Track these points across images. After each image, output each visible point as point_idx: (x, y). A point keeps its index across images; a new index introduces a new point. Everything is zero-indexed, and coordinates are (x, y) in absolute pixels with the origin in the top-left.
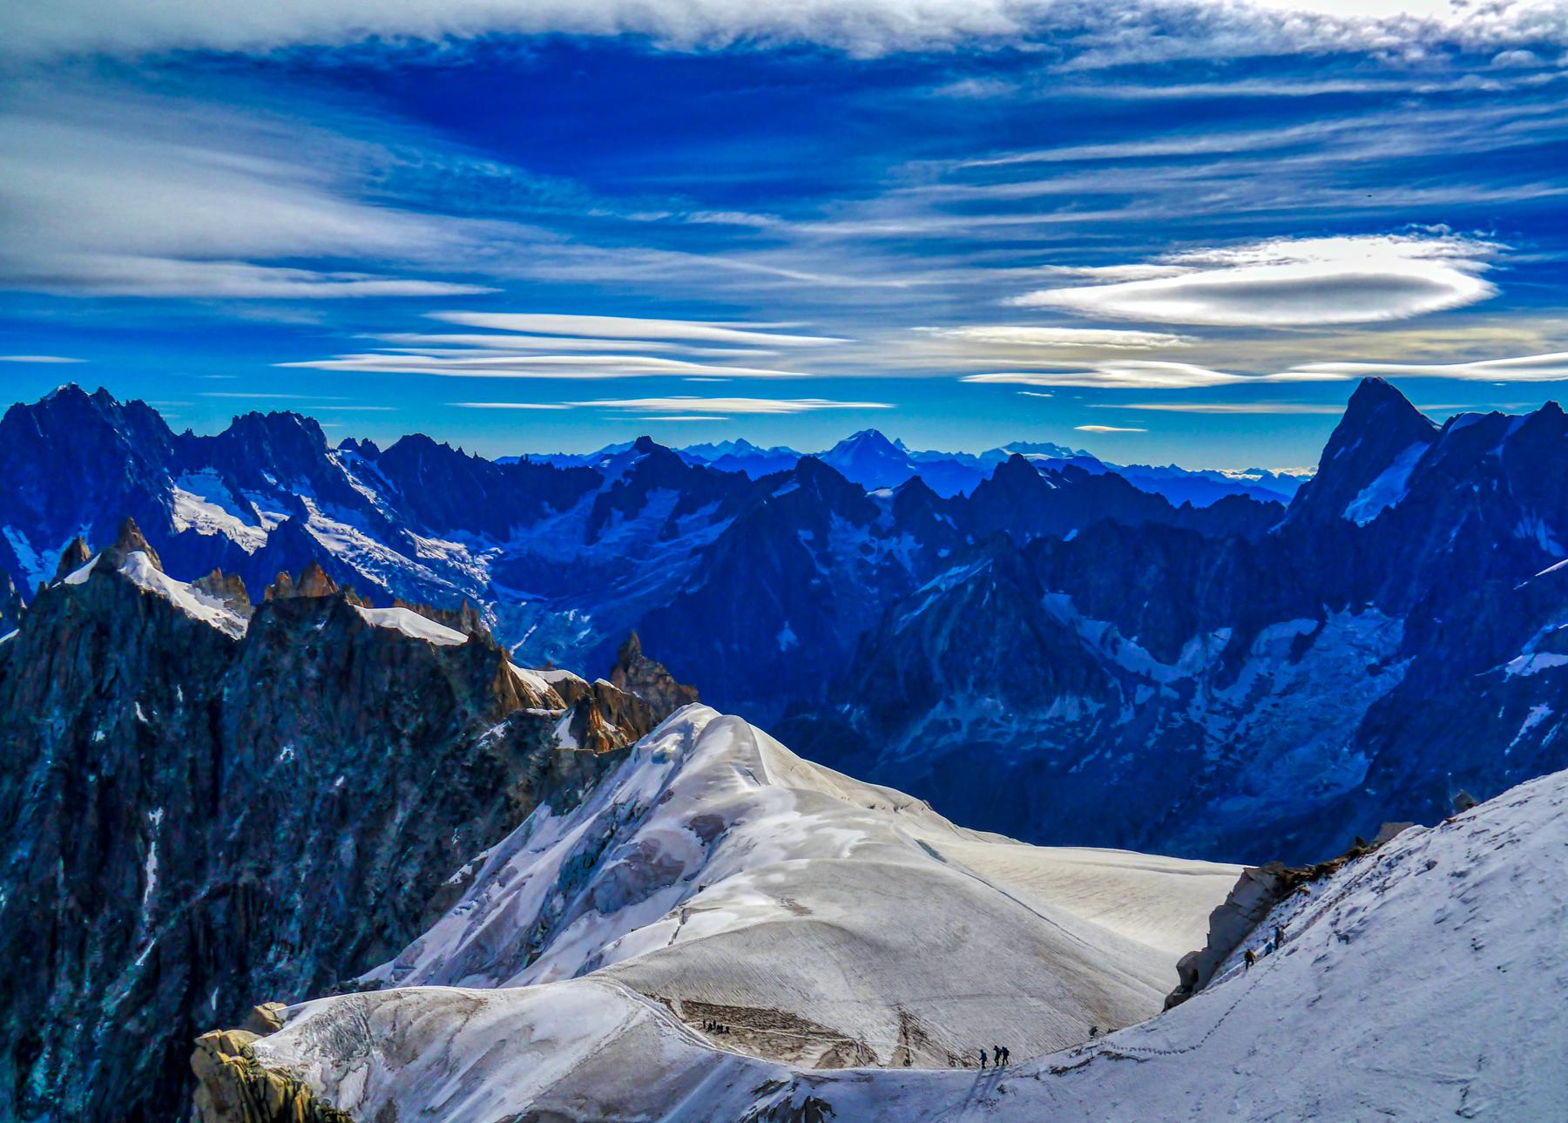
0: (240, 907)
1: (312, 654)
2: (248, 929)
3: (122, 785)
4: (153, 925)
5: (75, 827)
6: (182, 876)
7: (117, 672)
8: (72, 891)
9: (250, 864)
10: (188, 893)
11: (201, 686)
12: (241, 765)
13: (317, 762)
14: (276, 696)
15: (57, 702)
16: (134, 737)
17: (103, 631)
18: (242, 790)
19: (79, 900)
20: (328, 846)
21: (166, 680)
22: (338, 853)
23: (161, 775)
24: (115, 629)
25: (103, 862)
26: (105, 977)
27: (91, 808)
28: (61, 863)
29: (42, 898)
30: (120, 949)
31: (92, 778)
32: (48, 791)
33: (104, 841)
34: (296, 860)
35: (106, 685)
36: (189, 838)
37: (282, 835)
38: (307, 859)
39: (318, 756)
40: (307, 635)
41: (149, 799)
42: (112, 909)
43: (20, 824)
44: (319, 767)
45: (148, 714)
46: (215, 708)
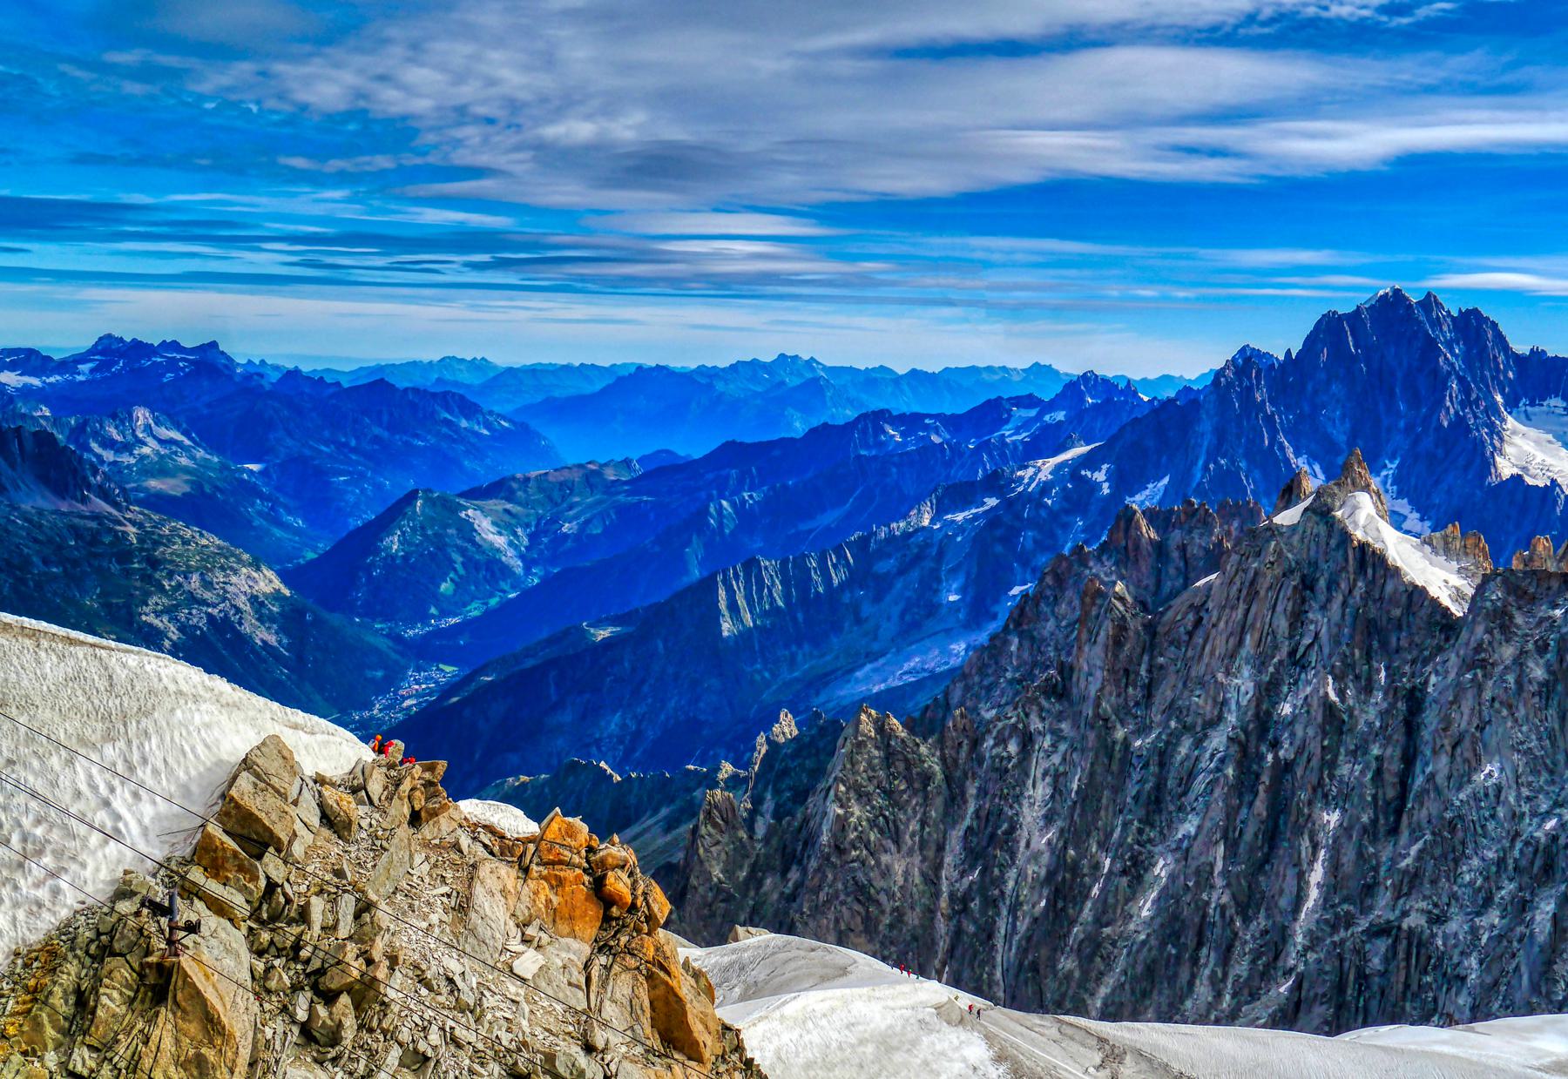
0: (1401, 955)
1: (1542, 649)
2: (1407, 986)
3: (1299, 773)
4: (1306, 949)
5: (1244, 810)
6: (1345, 900)
7: (1317, 634)
8: (1228, 885)
9: (1423, 905)
10: (1349, 921)
11: (1407, 668)
12: (1432, 776)
13: (1525, 792)
14: (1487, 695)
15: (1247, 663)
16: (1320, 719)
17: (1308, 584)
18: (1432, 807)
19: (1234, 897)
20: (1522, 907)
21: (1368, 657)
22: (1533, 919)
23: (1344, 770)
24: (1322, 583)
25: (1267, 860)
26: (1245, 997)
27: (1262, 794)
28: (1221, 849)
29: (1197, 884)
30: (1267, 966)
31: (1270, 757)
32: (1222, 761)
33: (1272, 835)
34: (1479, 914)
35: (1301, 650)
36: (1360, 854)
37: (1467, 878)
38: (1494, 917)
39: (1530, 784)
40: (1542, 620)
41: (1325, 796)
42: (1268, 917)
43: (1192, 796)
44: (1528, 799)
45: (1341, 693)
46: (1415, 700)
